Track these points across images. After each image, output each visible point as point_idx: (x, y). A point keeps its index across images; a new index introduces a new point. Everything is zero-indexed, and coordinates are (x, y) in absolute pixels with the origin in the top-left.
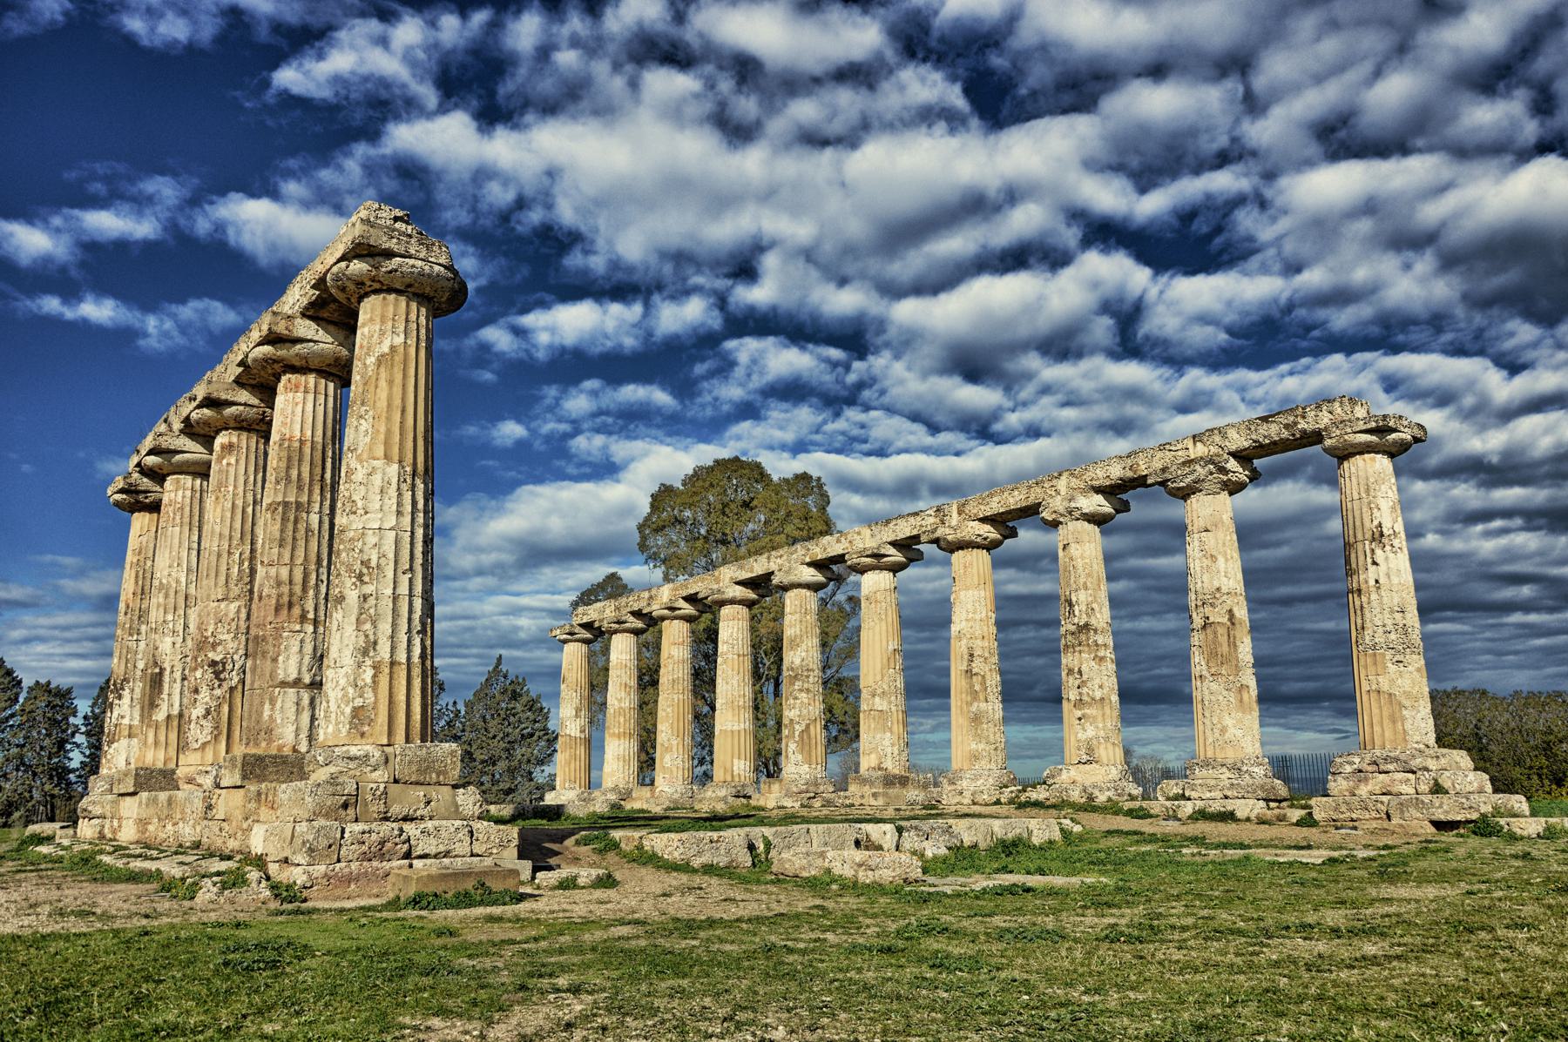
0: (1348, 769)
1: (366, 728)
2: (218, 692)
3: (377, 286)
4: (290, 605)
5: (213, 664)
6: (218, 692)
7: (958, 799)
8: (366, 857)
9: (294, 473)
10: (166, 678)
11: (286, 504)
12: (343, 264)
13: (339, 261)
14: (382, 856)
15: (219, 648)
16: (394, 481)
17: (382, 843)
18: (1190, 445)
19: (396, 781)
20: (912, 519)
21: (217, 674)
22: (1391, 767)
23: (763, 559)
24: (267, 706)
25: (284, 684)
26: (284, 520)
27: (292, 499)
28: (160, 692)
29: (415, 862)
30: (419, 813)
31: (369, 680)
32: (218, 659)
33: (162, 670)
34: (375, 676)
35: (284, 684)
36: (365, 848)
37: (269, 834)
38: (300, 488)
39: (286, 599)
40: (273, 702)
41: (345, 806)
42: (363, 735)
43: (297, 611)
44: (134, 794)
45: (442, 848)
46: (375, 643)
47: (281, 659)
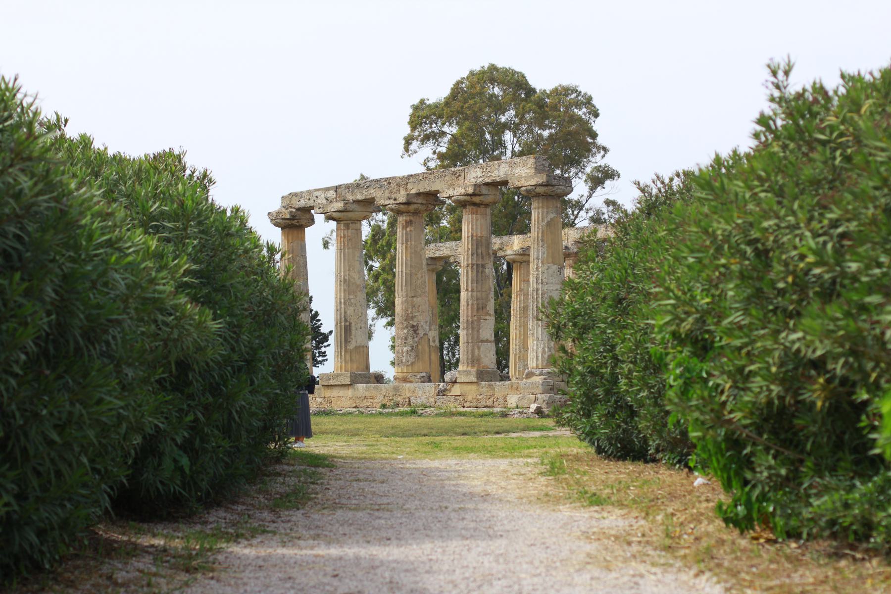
2: (416, 339)
5: (413, 326)
6: (416, 339)
9: (480, 251)
10: (353, 328)
11: (477, 265)
21: (415, 331)
24: (476, 350)
25: (482, 341)
26: (477, 272)
28: (350, 335)
33: (350, 324)
35: (482, 341)
38: (482, 258)
39: (480, 306)
40: (479, 348)
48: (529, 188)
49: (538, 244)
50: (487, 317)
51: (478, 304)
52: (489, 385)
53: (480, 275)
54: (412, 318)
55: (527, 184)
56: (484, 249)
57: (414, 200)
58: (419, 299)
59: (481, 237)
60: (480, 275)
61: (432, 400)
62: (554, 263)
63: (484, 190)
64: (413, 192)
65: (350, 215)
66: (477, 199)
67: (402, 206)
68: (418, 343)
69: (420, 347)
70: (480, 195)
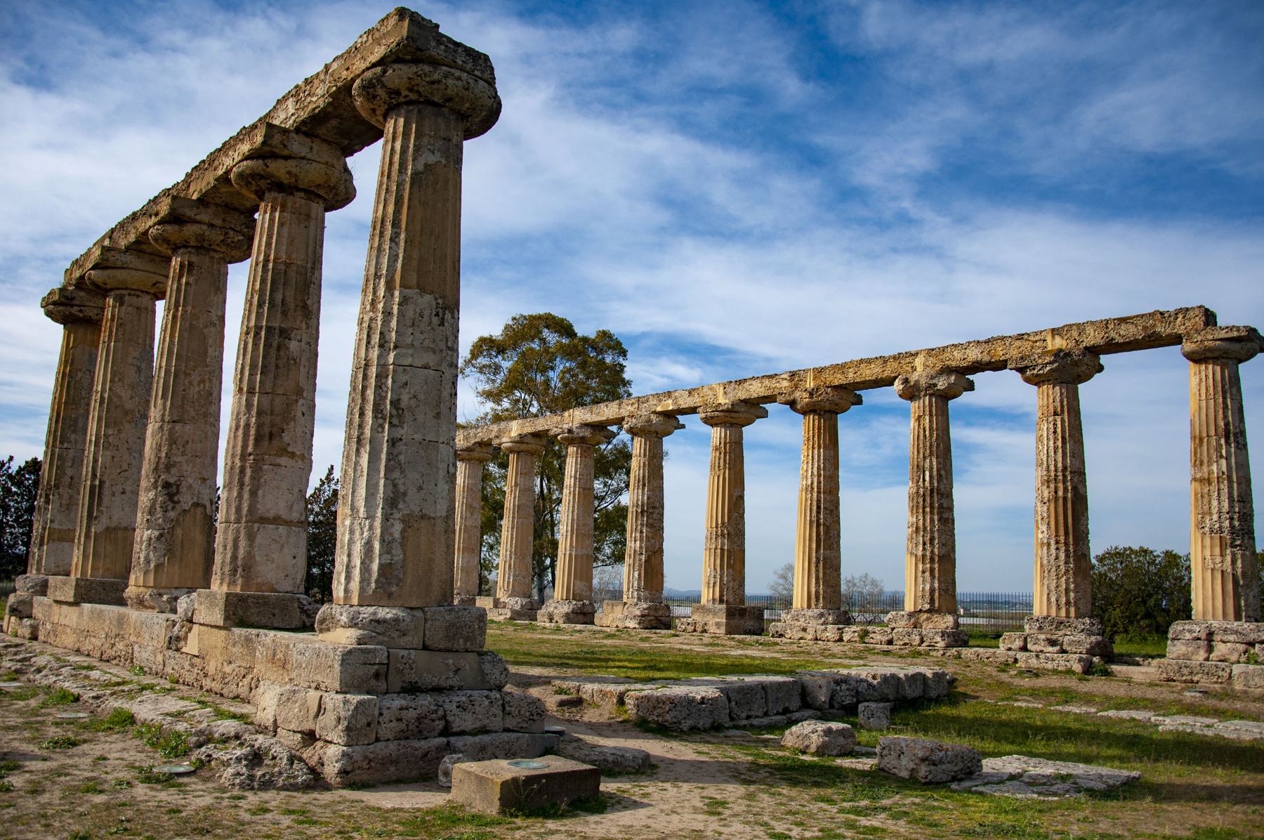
0: (1188, 636)
1: (394, 589)
2: (172, 514)
3: (413, 96)
4: (271, 436)
5: (167, 485)
6: (172, 514)
7: (801, 634)
8: (403, 736)
9: (279, 297)
10: (106, 491)
12: (379, 69)
13: (374, 65)
14: (420, 734)
15: (174, 471)
16: (427, 313)
17: (419, 719)
18: (1049, 339)
19: (425, 648)
20: (766, 382)
21: (171, 496)
22: (1232, 638)
23: (614, 405)
25: (263, 520)
27: (276, 324)
29: (452, 739)
30: (450, 682)
31: (397, 535)
32: (172, 480)
34: (403, 531)
35: (263, 520)
36: (403, 726)
37: (286, 699)
38: (284, 313)
39: (267, 430)
41: (377, 676)
42: (390, 595)
43: (276, 442)
44: (76, 604)
45: (478, 725)
46: (405, 494)
47: (260, 492)
48: (368, 74)
49: (382, 235)
50: (283, 461)
51: (259, 426)
52: (248, 640)
53: (273, 352)
54: (168, 467)
55: (363, 66)
56: (290, 294)
57: (189, 213)
58: (187, 427)
59: (288, 265)
60: (273, 352)
61: (160, 658)
62: (423, 290)
63: (298, 146)
64: (195, 197)
65: (120, 275)
66: (279, 169)
67: (168, 227)
68: (176, 522)
69: (179, 532)
70: (286, 158)
